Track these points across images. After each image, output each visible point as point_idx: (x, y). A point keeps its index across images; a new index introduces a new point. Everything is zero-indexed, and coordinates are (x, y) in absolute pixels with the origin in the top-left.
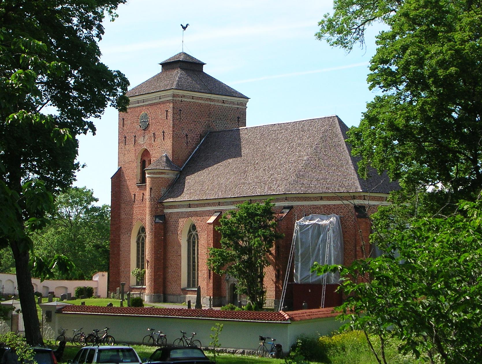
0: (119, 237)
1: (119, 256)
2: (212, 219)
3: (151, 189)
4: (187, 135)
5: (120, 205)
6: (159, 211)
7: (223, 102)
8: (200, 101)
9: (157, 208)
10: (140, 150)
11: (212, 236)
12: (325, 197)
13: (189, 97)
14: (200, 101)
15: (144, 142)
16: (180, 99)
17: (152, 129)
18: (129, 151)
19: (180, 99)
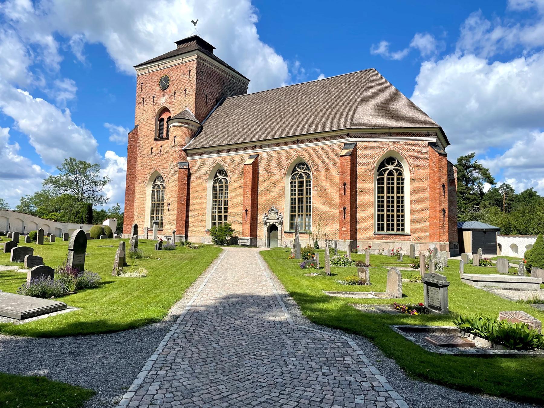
0: (134, 185)
1: (133, 202)
2: (251, 161)
3: (175, 137)
4: (207, 96)
5: (136, 158)
6: (183, 158)
7: (233, 77)
8: (217, 70)
9: (180, 155)
10: (158, 108)
11: (251, 176)
12: (394, 133)
13: (209, 63)
14: (217, 70)
15: (163, 101)
16: (202, 62)
17: (172, 88)
18: (148, 110)
19: (202, 62)
